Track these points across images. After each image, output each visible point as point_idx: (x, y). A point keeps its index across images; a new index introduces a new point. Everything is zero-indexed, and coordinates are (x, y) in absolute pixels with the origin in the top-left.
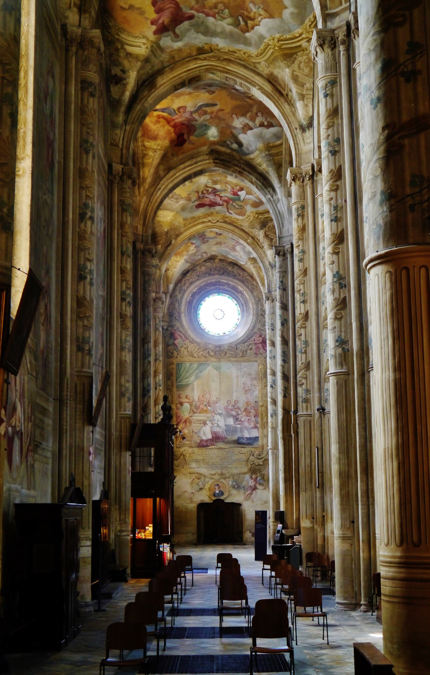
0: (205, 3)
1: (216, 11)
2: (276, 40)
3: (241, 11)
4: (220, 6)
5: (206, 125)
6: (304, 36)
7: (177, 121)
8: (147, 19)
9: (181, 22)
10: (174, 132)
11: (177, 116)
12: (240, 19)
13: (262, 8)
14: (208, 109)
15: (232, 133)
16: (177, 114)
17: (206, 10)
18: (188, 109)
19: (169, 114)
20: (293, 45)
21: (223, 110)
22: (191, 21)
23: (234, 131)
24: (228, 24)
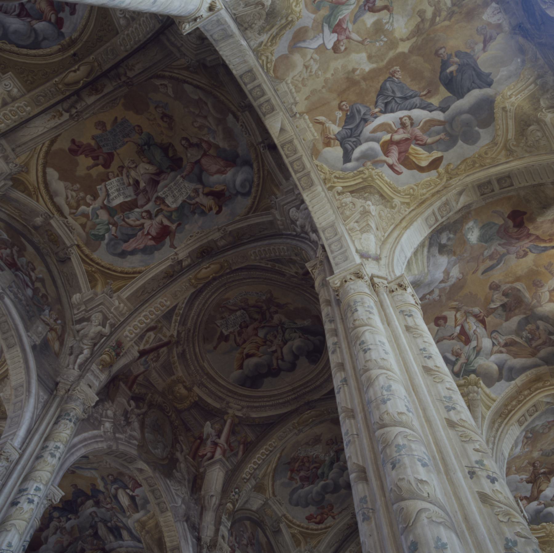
1: (549, 426)
5: (486, 242)
7: (527, 241)
10: (529, 230)
11: (527, 246)
14: (489, 263)
15: (454, 254)
16: (527, 248)
18: (513, 256)
19: (537, 246)
21: (473, 273)
23: (454, 258)
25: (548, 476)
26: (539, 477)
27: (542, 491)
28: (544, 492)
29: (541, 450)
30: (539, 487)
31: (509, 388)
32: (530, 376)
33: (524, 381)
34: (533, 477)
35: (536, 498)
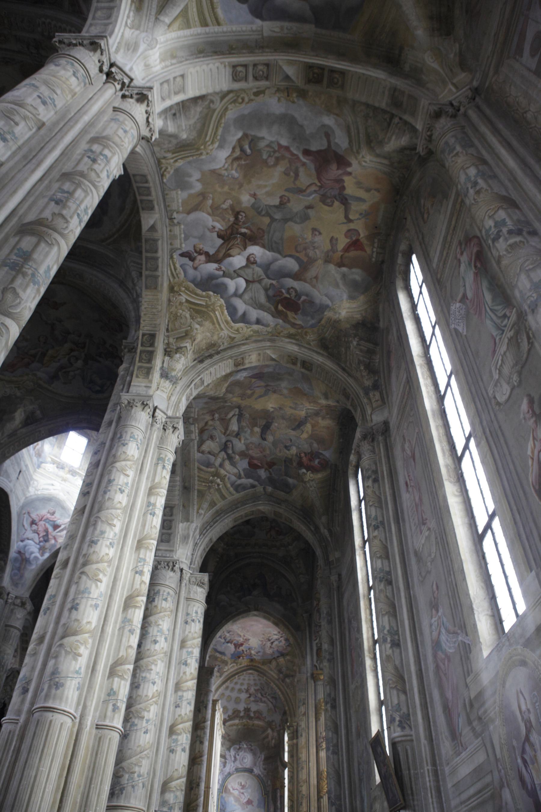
0: (288, 165)
1: (277, 155)
2: (205, 153)
3: (247, 162)
4: (271, 161)
6: (172, 161)
8: (355, 178)
9: (319, 152)
12: (249, 151)
13: (223, 176)
17: (287, 155)
20: (182, 153)
22: (307, 147)
24: (263, 138)
25: (247, 241)
26: (236, 237)
27: (230, 256)
28: (231, 258)
29: (254, 195)
30: (229, 249)
31: (249, 27)
32: (286, 31)
33: (275, 35)
34: (228, 232)
35: (219, 261)
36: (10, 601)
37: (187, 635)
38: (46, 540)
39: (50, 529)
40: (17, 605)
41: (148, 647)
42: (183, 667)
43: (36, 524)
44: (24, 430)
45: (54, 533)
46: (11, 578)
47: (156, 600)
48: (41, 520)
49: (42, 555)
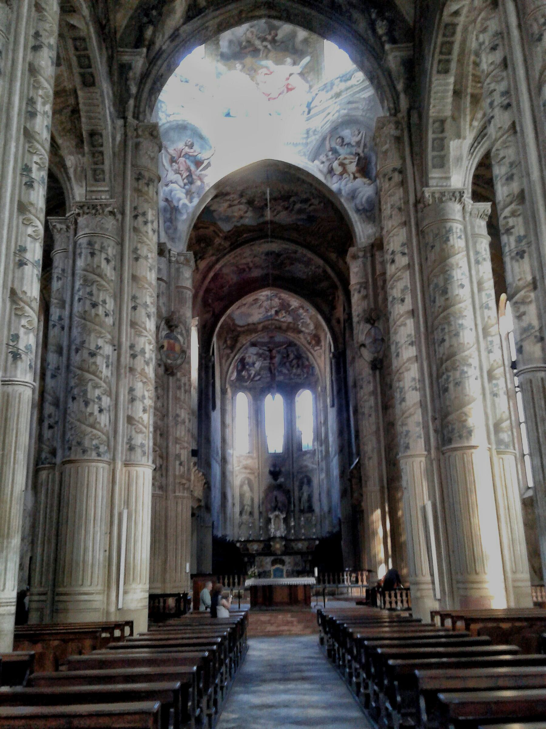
36: (173, 259)
37: (482, 277)
38: (191, 183)
39: (193, 168)
40: (181, 263)
41: (456, 292)
42: (486, 311)
43: (176, 162)
44: (187, 28)
45: (198, 172)
46: (166, 233)
47: (451, 238)
48: (180, 157)
49: (191, 202)
